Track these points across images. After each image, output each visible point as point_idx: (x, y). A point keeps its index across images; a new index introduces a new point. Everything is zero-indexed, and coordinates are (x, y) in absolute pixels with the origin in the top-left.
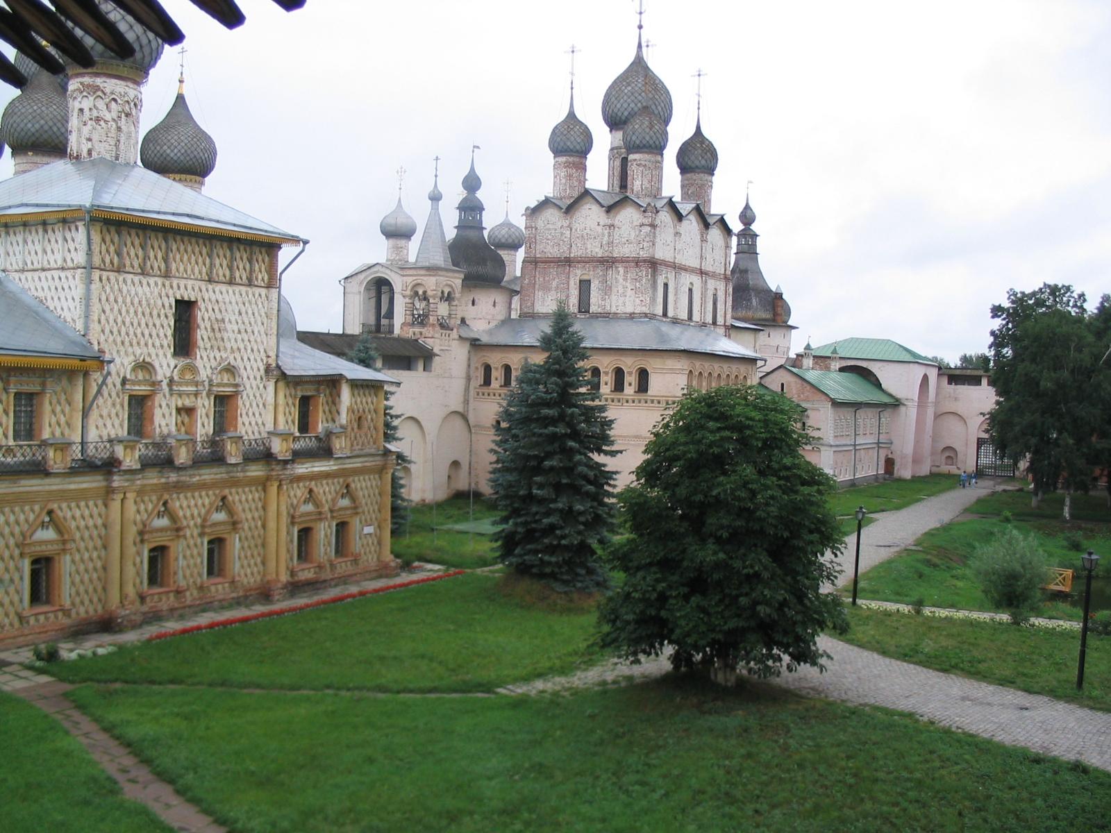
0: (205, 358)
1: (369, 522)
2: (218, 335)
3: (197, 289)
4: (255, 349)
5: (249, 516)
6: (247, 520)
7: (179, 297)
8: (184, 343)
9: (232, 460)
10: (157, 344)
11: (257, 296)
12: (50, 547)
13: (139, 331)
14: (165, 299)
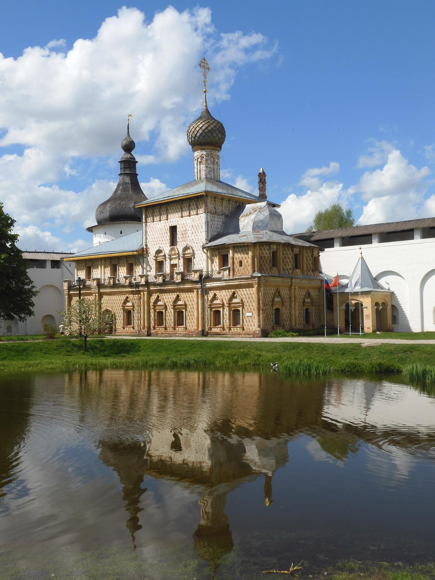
0: (181, 245)
1: (250, 310)
2: (185, 236)
3: (176, 221)
4: (199, 238)
5: (190, 304)
6: (190, 305)
7: (170, 226)
8: (173, 241)
9: (178, 281)
10: (165, 243)
11: (199, 218)
12: (129, 308)
13: (159, 240)
14: (166, 227)
